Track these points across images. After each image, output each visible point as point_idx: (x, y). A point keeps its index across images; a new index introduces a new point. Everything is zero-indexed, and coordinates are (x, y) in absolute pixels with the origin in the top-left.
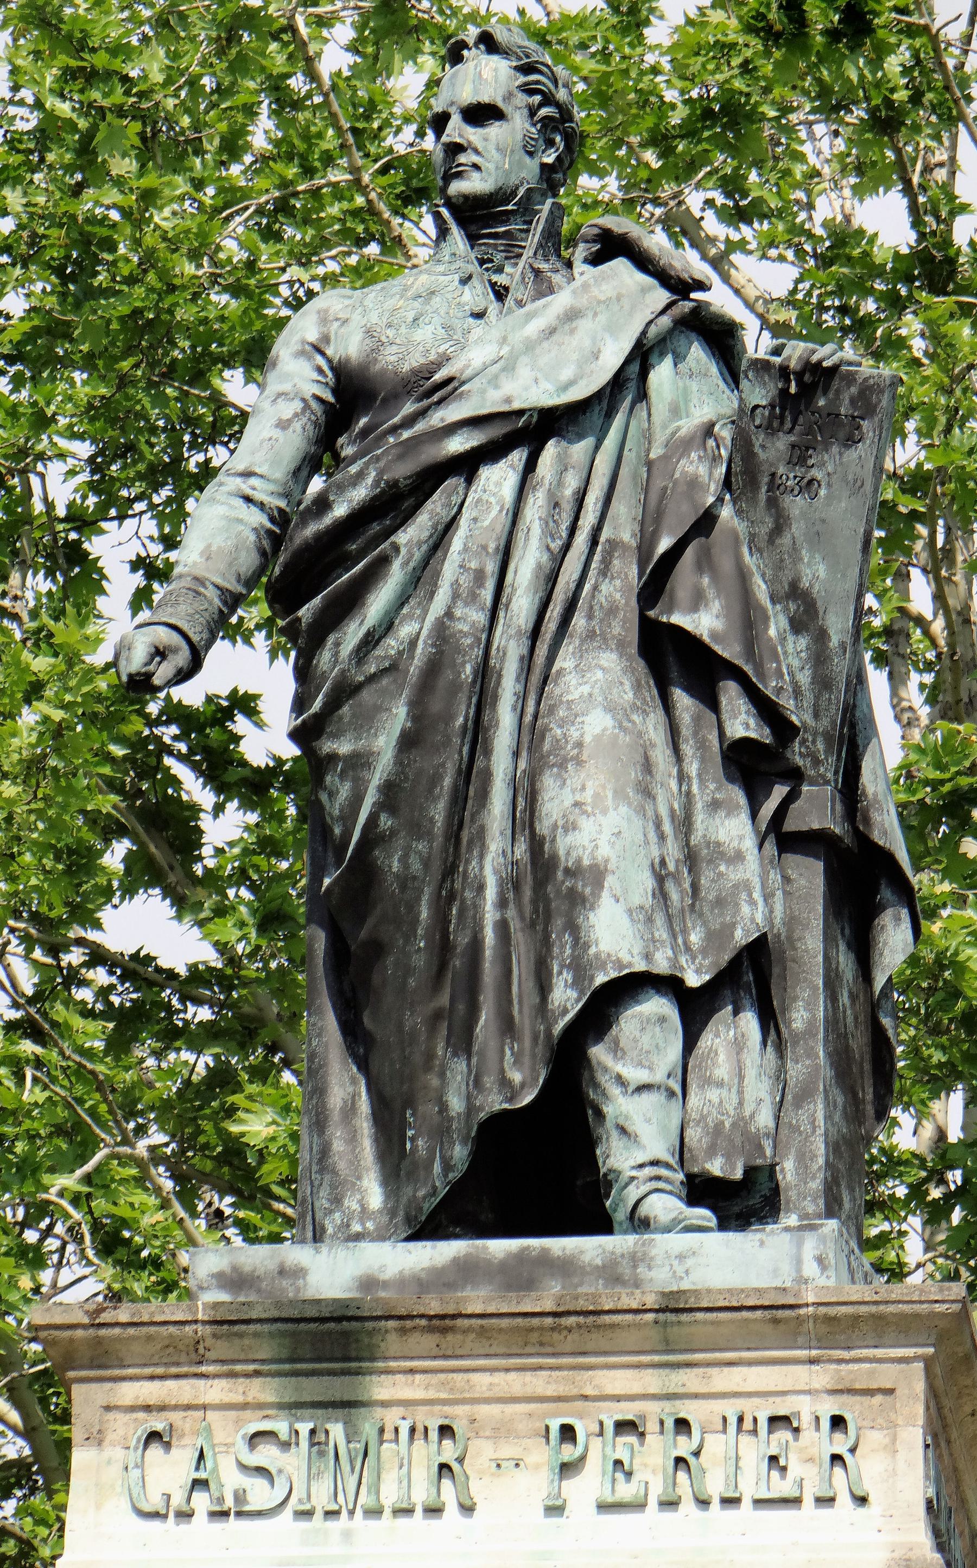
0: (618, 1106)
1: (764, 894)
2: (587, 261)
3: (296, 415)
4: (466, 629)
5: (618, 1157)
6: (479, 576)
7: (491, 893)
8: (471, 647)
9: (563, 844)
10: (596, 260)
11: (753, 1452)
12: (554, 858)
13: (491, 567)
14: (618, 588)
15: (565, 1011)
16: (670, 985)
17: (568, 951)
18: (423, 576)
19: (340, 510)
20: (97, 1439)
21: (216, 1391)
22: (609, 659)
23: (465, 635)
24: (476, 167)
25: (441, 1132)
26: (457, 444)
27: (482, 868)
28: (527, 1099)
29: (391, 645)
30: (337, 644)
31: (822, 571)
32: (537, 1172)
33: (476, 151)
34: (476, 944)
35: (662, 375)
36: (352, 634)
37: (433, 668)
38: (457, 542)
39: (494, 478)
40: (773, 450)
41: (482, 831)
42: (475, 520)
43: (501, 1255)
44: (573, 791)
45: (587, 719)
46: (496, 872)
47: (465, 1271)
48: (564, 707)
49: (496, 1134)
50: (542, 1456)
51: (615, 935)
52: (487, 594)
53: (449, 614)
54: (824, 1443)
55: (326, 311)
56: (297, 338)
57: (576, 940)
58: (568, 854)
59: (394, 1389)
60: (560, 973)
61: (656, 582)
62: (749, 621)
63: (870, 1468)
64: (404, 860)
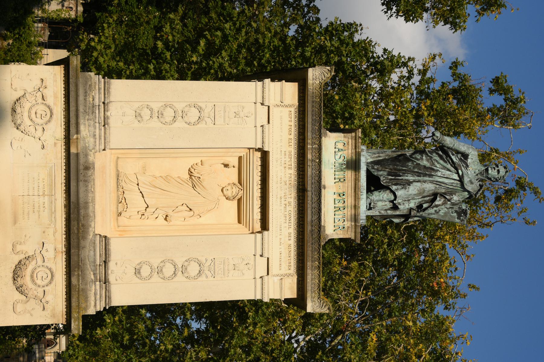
1: (404, 208)
6: (444, 175)
7: (406, 178)
10: (480, 185)
11: (340, 217)
16: (395, 199)
18: (445, 168)
20: (345, 137)
21: (350, 151)
29: (436, 164)
34: (400, 176)
35: (466, 193)
36: (438, 158)
37: (433, 169)
49: (377, 179)
59: (349, 174)
61: (442, 195)
62: (437, 206)
63: (338, 231)
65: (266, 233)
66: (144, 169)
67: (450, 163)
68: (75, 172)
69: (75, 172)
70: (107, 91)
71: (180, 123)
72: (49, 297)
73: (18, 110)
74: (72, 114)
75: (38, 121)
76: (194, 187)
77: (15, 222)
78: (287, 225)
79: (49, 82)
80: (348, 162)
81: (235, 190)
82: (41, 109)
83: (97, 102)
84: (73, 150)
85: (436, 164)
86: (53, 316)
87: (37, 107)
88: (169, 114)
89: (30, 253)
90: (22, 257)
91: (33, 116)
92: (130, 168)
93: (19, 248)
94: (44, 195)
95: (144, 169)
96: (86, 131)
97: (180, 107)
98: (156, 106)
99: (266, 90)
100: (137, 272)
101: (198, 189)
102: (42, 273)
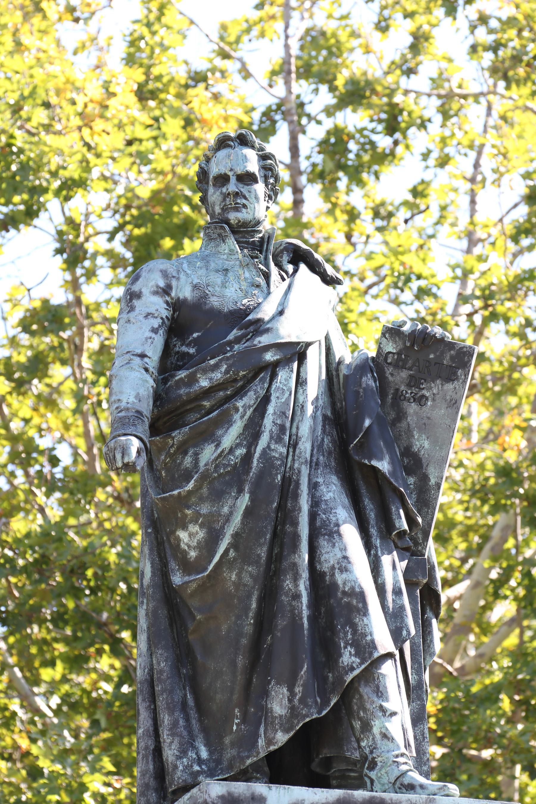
2: (289, 262)
3: (160, 326)
4: (277, 456)
6: (282, 428)
8: (280, 466)
9: (340, 578)
12: (334, 585)
13: (288, 425)
15: (352, 669)
17: (350, 636)
19: (204, 383)
22: (334, 479)
23: (277, 459)
24: (245, 206)
26: (269, 357)
27: (297, 586)
28: (324, 713)
30: (196, 456)
31: (426, 444)
33: (246, 198)
37: (261, 475)
38: (271, 409)
39: (284, 377)
40: (399, 378)
41: (294, 566)
42: (278, 397)
43: (360, 800)
44: (341, 550)
45: (337, 511)
46: (306, 589)
48: (323, 503)
52: (287, 438)
53: (268, 447)
55: (166, 271)
56: (153, 283)
57: (355, 631)
58: (344, 584)
60: (345, 647)
64: (239, 575)
67: (228, 399)
85: (233, 460)
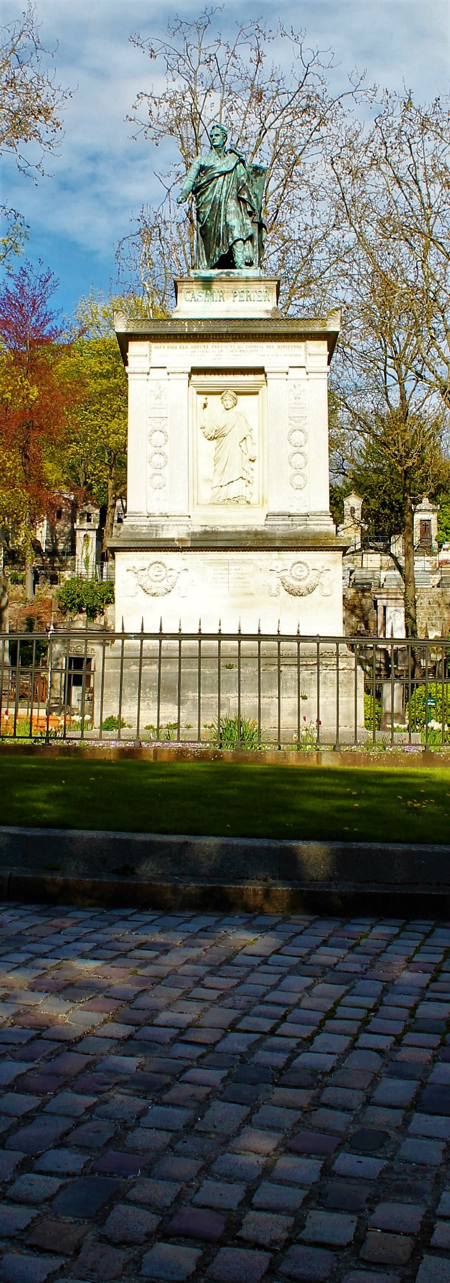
0: (237, 254)
1: (252, 229)
5: (236, 259)
14: (234, 192)
16: (242, 240)
18: (213, 191)
21: (195, 287)
25: (215, 256)
26: (216, 175)
32: (227, 262)
36: (204, 197)
40: (252, 177)
47: (222, 273)
50: (232, 295)
51: (236, 234)
54: (264, 294)
59: (216, 286)
61: (239, 192)
62: (249, 196)
65: (266, 370)
66: (207, 480)
68: (208, 542)
69: (208, 542)
70: (135, 514)
71: (166, 449)
72: (318, 566)
73: (154, 591)
74: (162, 544)
75: (163, 573)
76: (224, 436)
77: (252, 594)
78: (259, 350)
79: (129, 565)
80: (203, 289)
81: (227, 397)
82: (153, 571)
83: (147, 523)
84: (189, 544)
86: (335, 562)
87: (151, 575)
88: (158, 459)
89: (280, 581)
90: (282, 589)
91: (159, 578)
92: (206, 493)
93: (274, 591)
94: (228, 570)
95: (207, 480)
96: (173, 532)
97: (151, 450)
98: (150, 471)
99: (136, 370)
100: (299, 488)
101: (226, 432)
102: (297, 571)
